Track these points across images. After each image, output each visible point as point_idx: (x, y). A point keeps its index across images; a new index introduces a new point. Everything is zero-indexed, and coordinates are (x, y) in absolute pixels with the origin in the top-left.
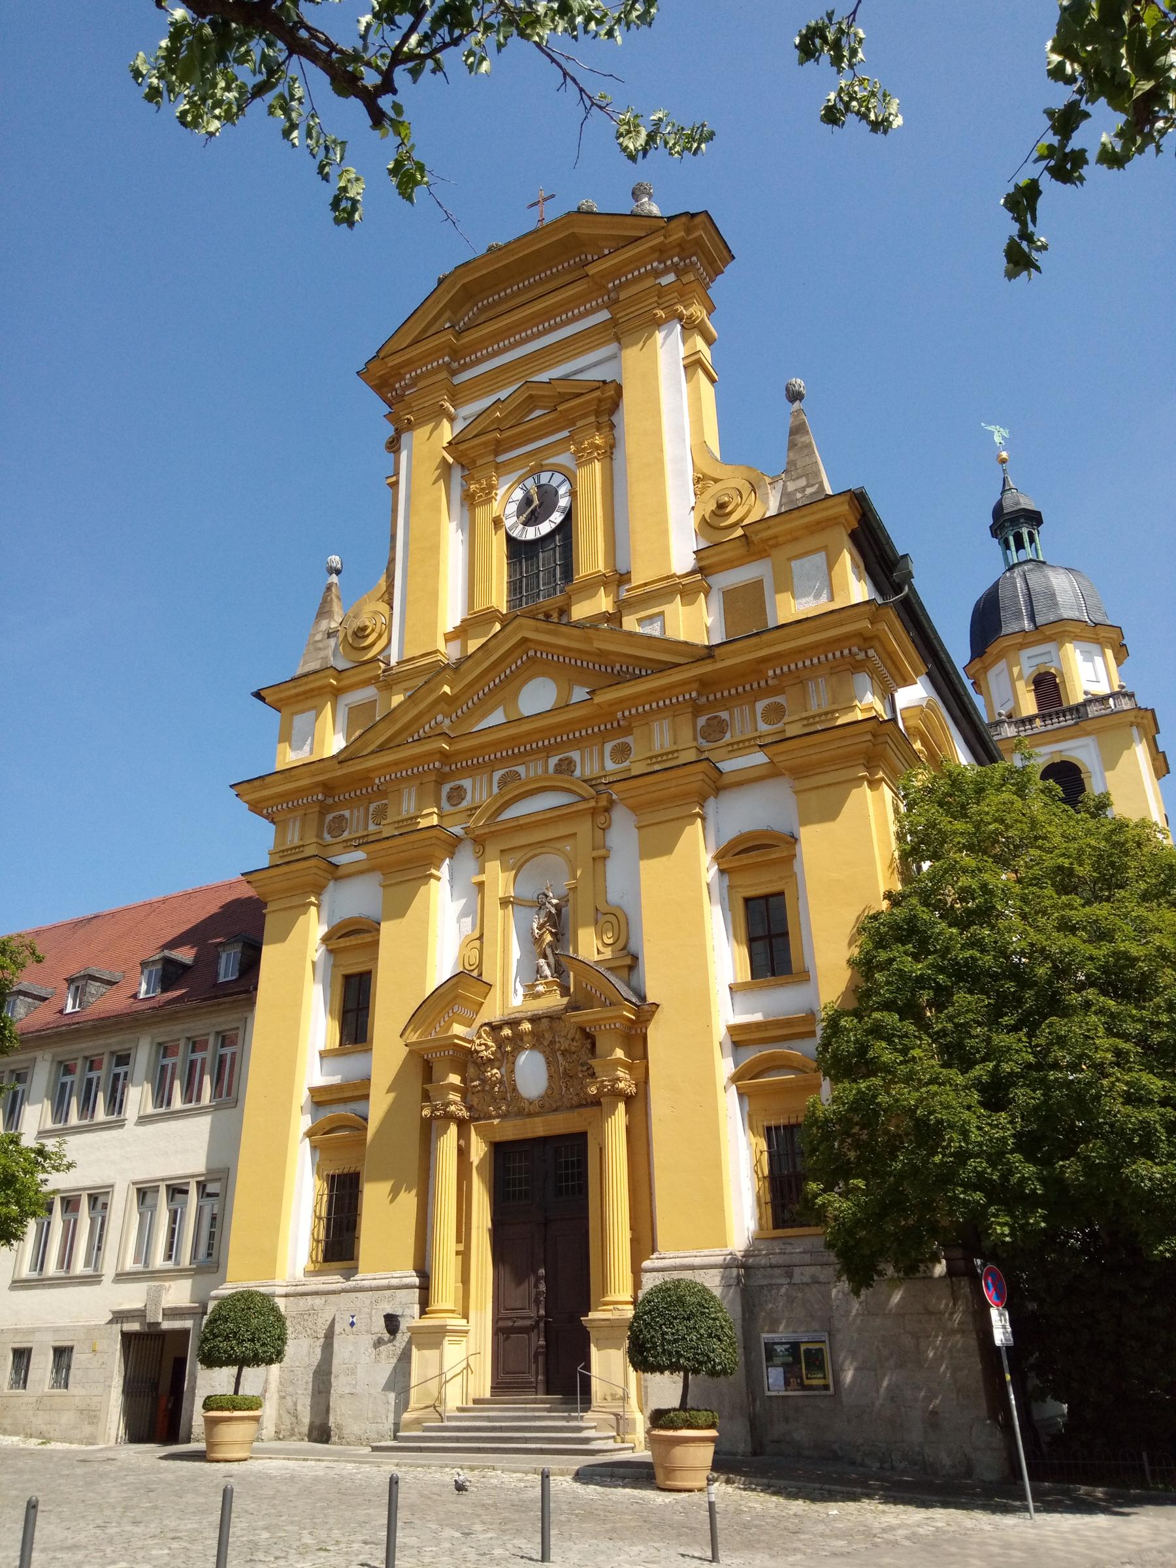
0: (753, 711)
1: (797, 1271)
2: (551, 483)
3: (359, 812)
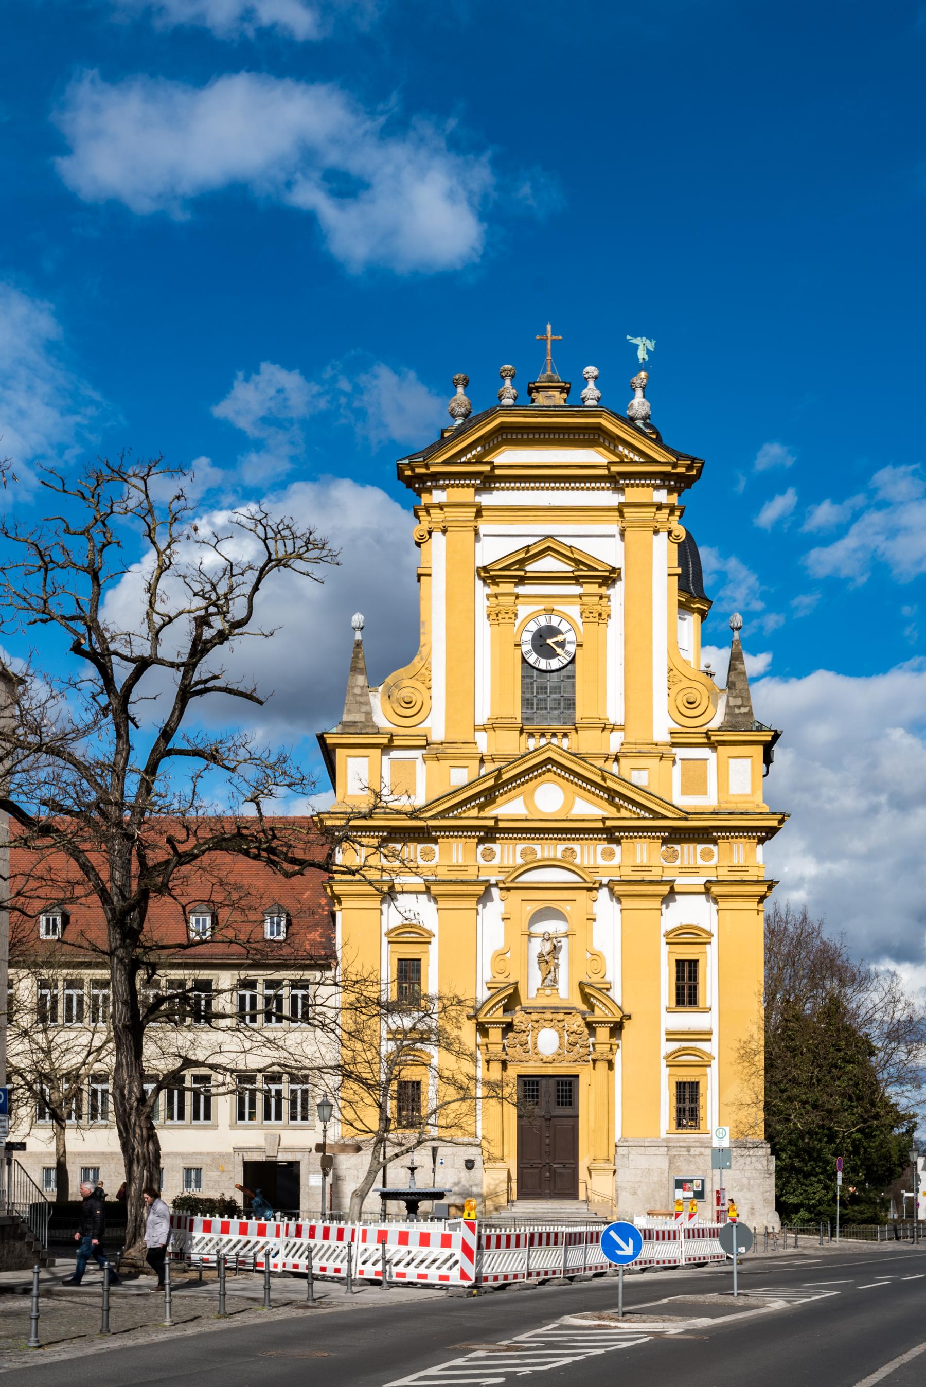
0: (695, 849)
1: (692, 1149)
2: (561, 627)
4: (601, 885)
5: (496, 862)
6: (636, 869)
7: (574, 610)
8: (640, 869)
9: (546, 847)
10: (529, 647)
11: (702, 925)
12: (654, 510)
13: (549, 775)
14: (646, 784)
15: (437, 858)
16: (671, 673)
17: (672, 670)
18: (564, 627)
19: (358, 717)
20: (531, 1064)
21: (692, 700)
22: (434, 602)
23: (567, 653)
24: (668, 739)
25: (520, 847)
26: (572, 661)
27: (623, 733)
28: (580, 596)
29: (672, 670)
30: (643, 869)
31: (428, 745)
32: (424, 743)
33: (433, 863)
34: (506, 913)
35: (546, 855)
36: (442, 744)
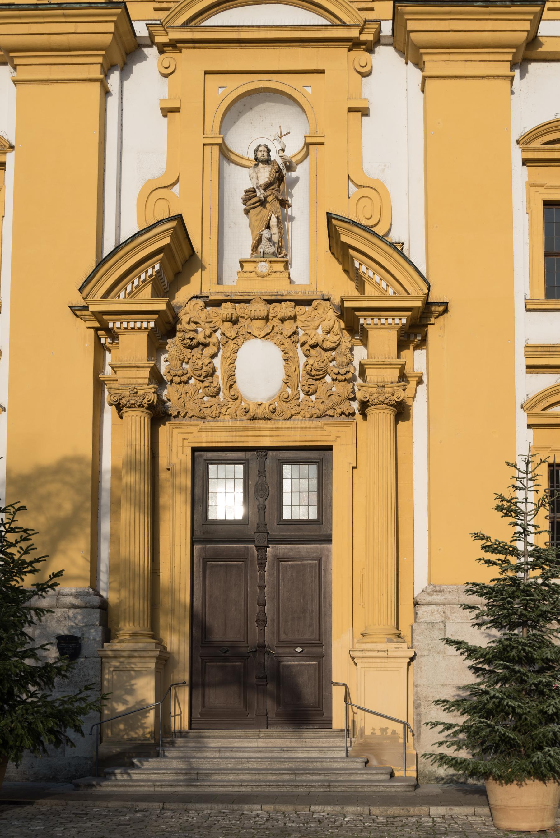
20: (224, 423)
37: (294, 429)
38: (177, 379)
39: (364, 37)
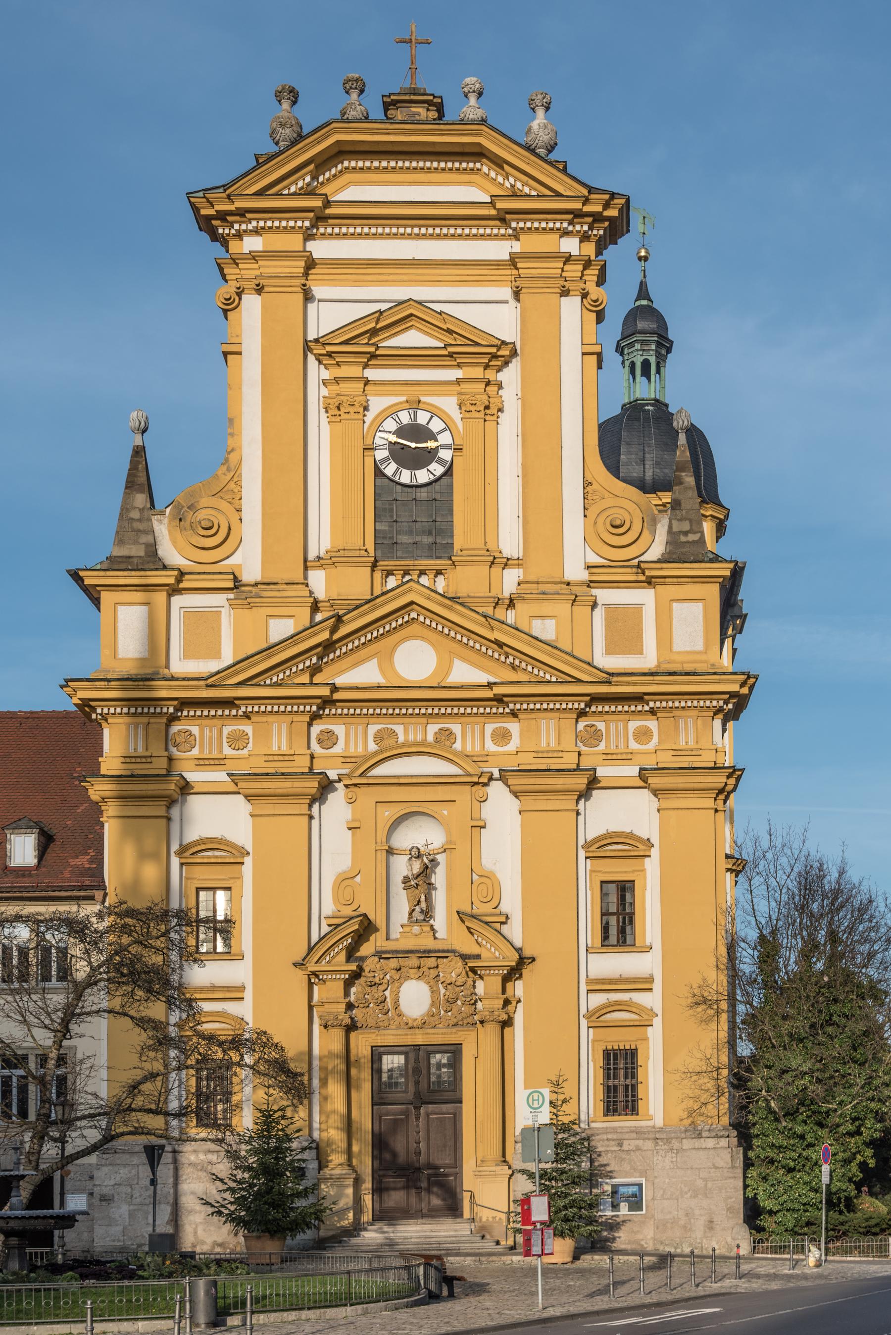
2: (430, 426)
3: (211, 731)
4: (491, 779)
5: (338, 749)
6: (540, 755)
7: (449, 404)
8: (545, 755)
9: (411, 728)
10: (386, 453)
11: (637, 832)
12: (561, 265)
13: (414, 628)
14: (554, 638)
15: (250, 745)
16: (589, 489)
17: (590, 484)
18: (436, 425)
19: (138, 551)
21: (618, 523)
22: (245, 389)
23: (441, 462)
24: (584, 576)
25: (373, 729)
26: (449, 472)
27: (521, 570)
28: (458, 382)
29: (590, 484)
30: (550, 755)
31: (236, 587)
32: (231, 584)
33: (245, 752)
34: (353, 820)
35: (411, 738)
36: (256, 584)
37: (438, 1034)
38: (362, 1006)
39: (481, 780)
